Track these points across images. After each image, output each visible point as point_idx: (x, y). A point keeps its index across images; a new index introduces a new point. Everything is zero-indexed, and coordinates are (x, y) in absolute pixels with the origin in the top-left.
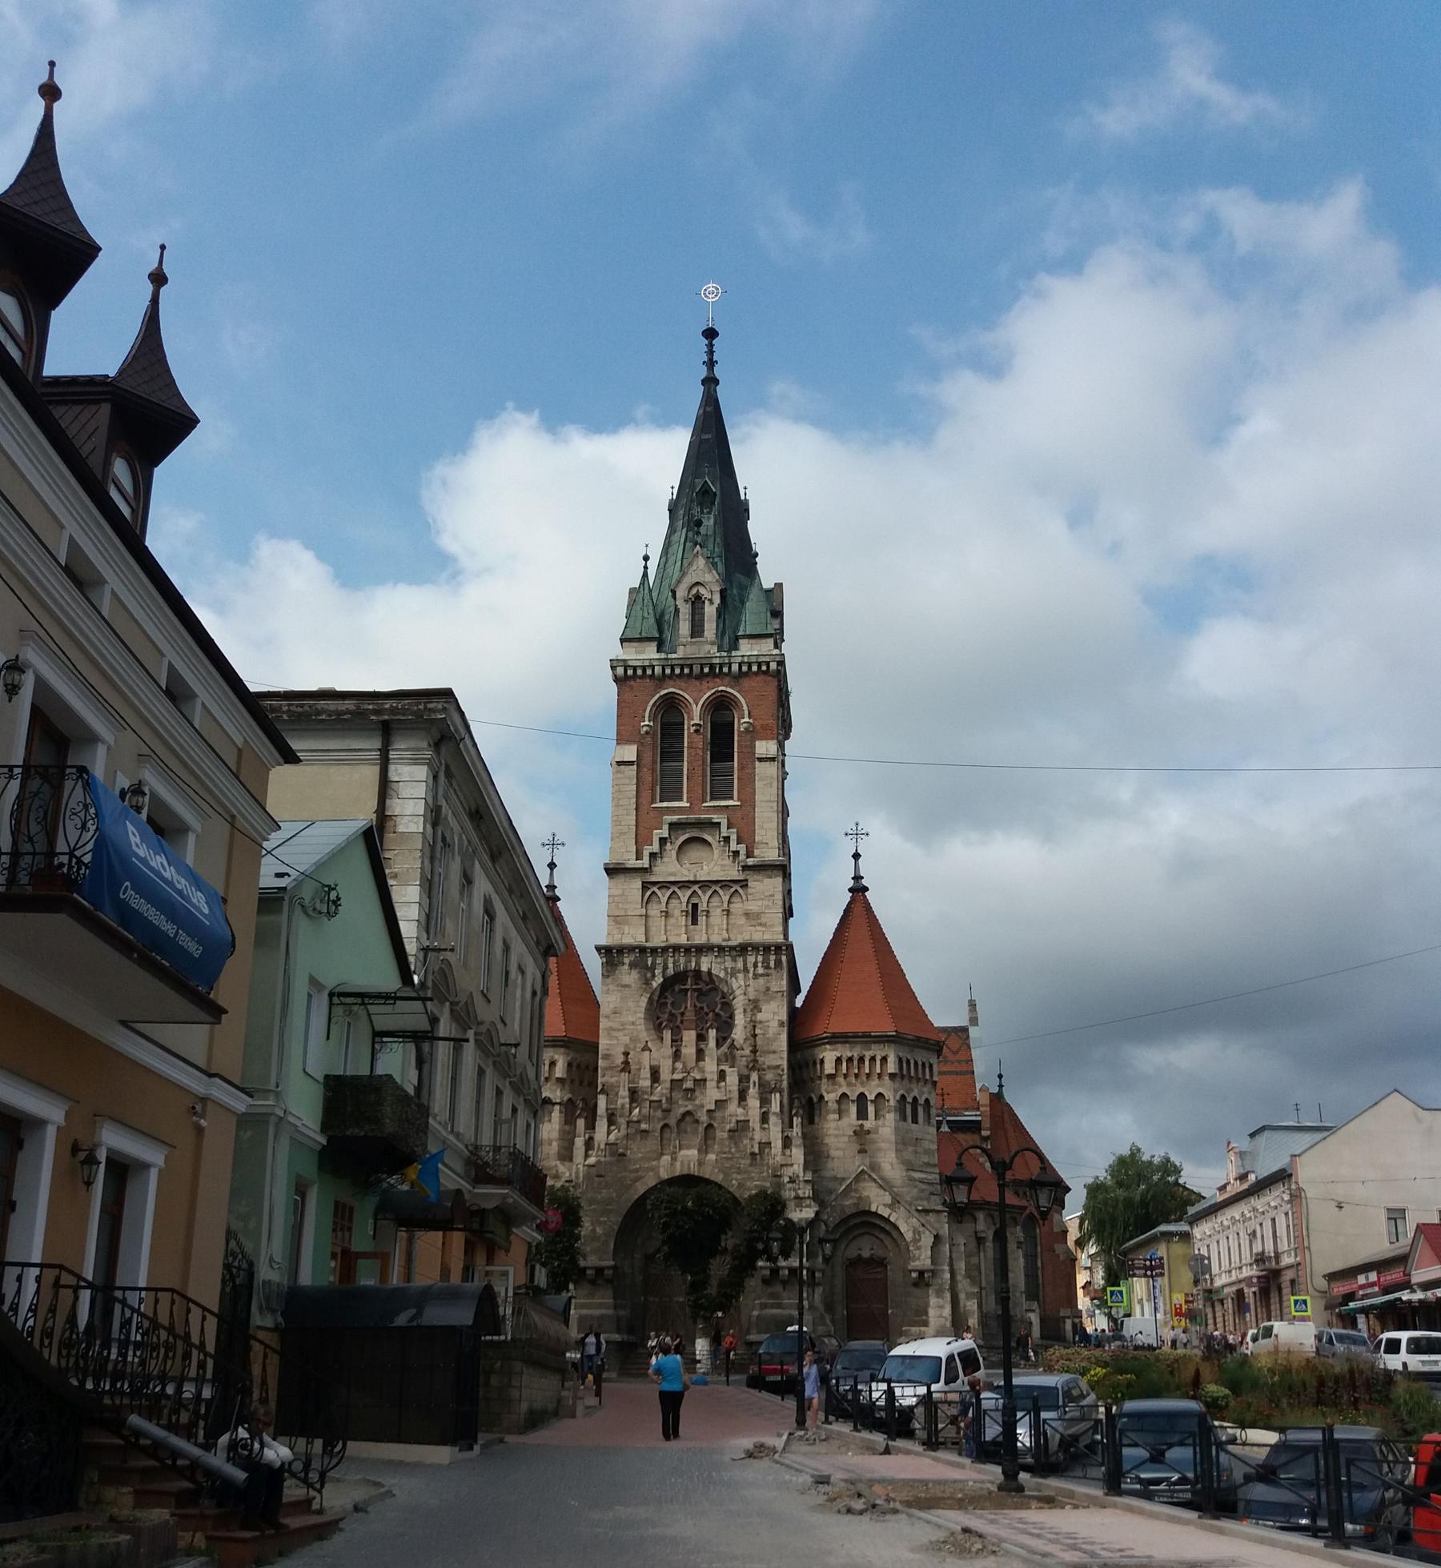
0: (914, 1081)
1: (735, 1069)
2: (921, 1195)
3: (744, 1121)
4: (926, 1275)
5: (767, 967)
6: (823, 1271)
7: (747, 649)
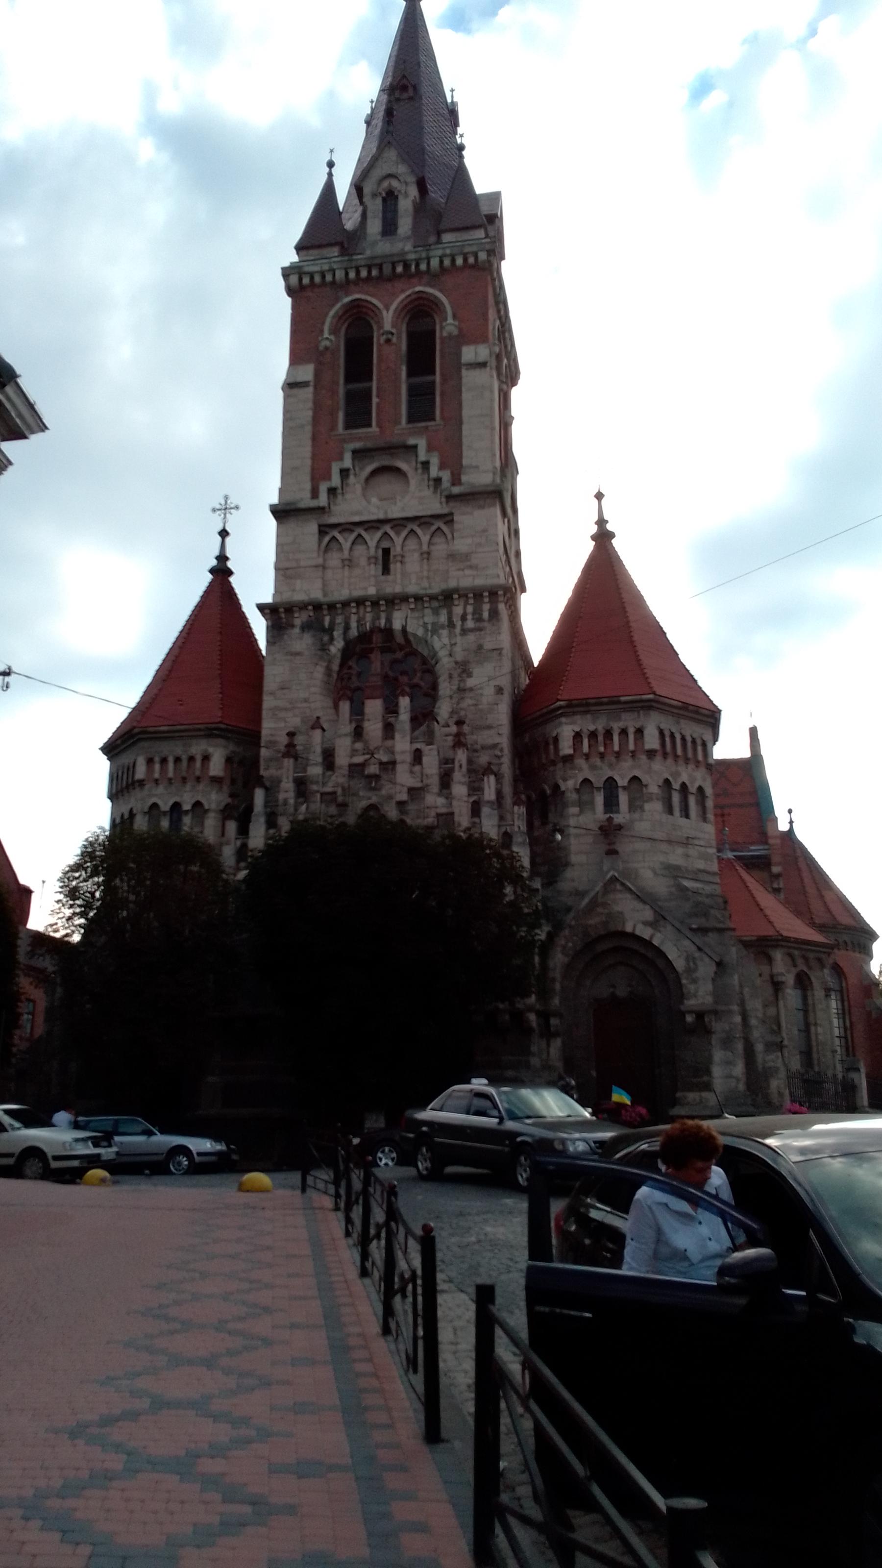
0: (681, 761)
5: (479, 619)
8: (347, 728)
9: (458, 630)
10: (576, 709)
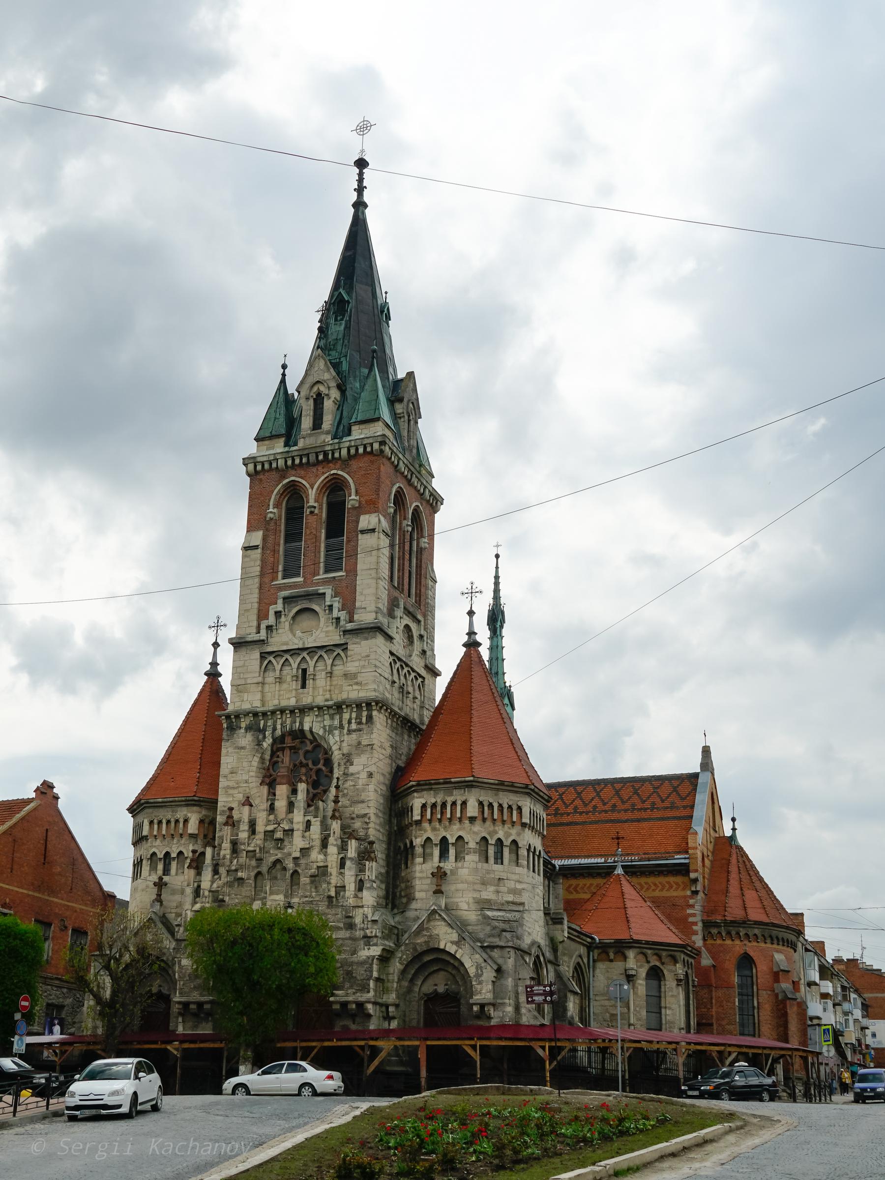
0: (499, 823)
1: (319, 819)
2: (493, 932)
3: (323, 867)
5: (360, 723)
6: (397, 1006)
7: (358, 433)
8: (265, 805)
10: (423, 787)
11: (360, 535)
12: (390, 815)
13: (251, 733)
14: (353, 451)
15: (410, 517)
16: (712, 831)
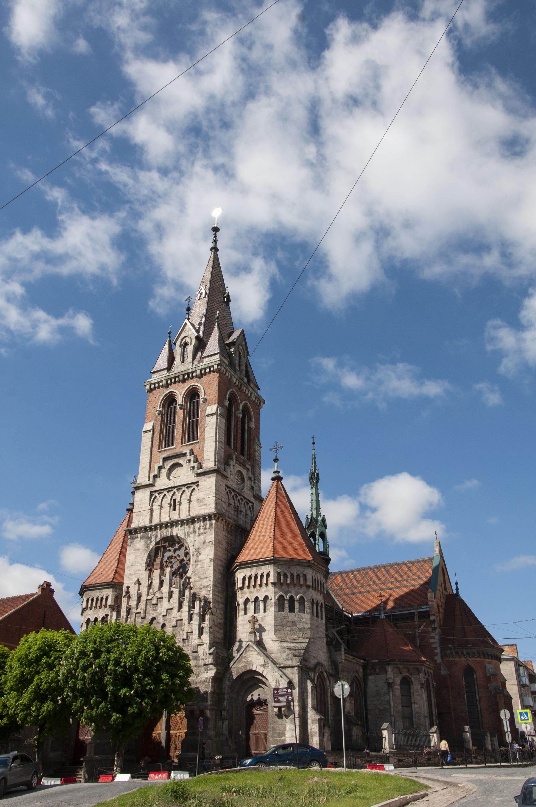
4: (283, 709)
5: (205, 529)
8: (147, 584)
9: (197, 533)
11: (207, 418)
12: (227, 586)
13: (144, 540)
14: (203, 372)
15: (241, 408)
16: (444, 591)
